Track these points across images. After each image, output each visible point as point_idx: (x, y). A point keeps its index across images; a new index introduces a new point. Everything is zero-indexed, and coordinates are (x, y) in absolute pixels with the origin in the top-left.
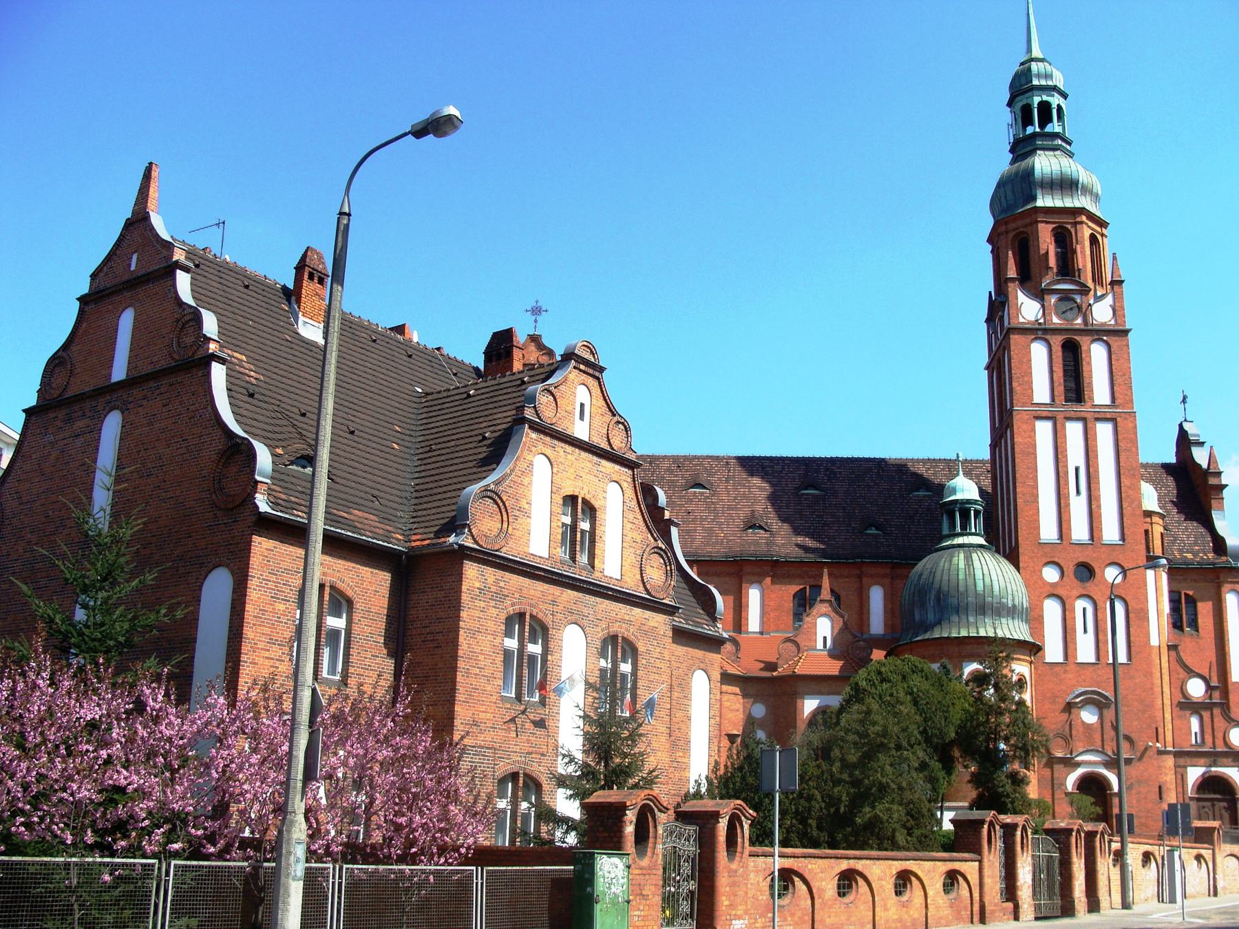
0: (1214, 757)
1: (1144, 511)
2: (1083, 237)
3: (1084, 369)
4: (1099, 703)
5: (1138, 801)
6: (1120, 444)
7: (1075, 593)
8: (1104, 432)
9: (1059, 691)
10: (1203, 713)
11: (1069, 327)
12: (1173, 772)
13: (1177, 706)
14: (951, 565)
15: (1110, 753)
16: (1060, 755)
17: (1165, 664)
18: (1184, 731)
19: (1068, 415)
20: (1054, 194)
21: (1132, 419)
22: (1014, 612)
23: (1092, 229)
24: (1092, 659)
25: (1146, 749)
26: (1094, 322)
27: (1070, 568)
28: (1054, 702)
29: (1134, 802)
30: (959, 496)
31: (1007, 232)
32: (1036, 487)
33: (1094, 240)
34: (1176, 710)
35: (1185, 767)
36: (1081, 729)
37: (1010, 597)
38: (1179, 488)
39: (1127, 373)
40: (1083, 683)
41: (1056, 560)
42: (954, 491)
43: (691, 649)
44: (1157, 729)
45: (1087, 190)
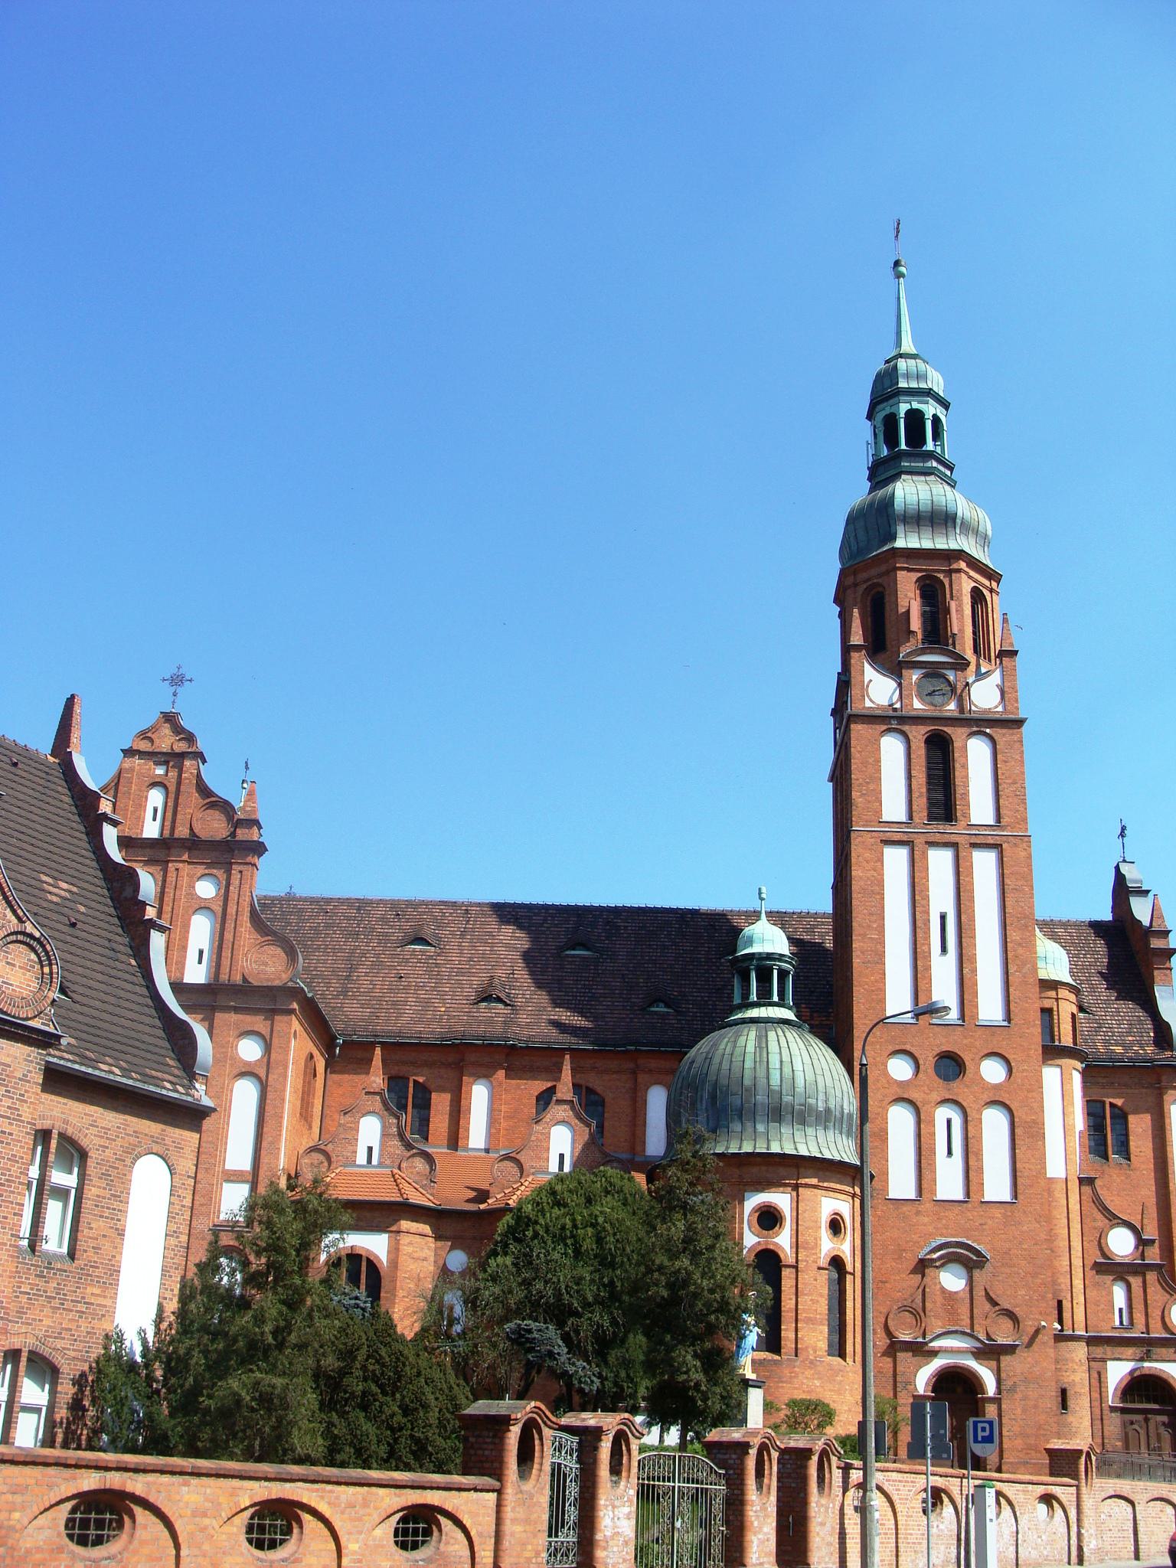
0: (1147, 1346)
1: (1041, 981)
2: (960, 590)
3: (957, 773)
4: (971, 1261)
5: (1024, 1411)
6: (1007, 881)
7: (936, 1096)
8: (984, 864)
9: (907, 1242)
10: (1131, 1279)
11: (937, 714)
12: (1085, 1368)
13: (1091, 1269)
14: (735, 1047)
15: (982, 1337)
16: (907, 1338)
17: (1075, 1206)
18: (1102, 1306)
20: (922, 532)
21: (1024, 845)
22: (825, 1118)
23: (976, 581)
24: (959, 1194)
25: (1037, 1332)
26: (973, 708)
27: (928, 1061)
28: (900, 1257)
29: (1019, 1411)
30: (756, 949)
31: (856, 585)
32: (882, 943)
33: (977, 596)
34: (1091, 1274)
35: (1104, 1360)
36: (939, 1299)
37: (821, 1097)
38: (1111, 956)
39: (1019, 780)
40: (944, 1231)
41: (908, 1047)
42: (750, 941)
43: (134, 1120)
44: (1060, 1303)
45: (967, 528)
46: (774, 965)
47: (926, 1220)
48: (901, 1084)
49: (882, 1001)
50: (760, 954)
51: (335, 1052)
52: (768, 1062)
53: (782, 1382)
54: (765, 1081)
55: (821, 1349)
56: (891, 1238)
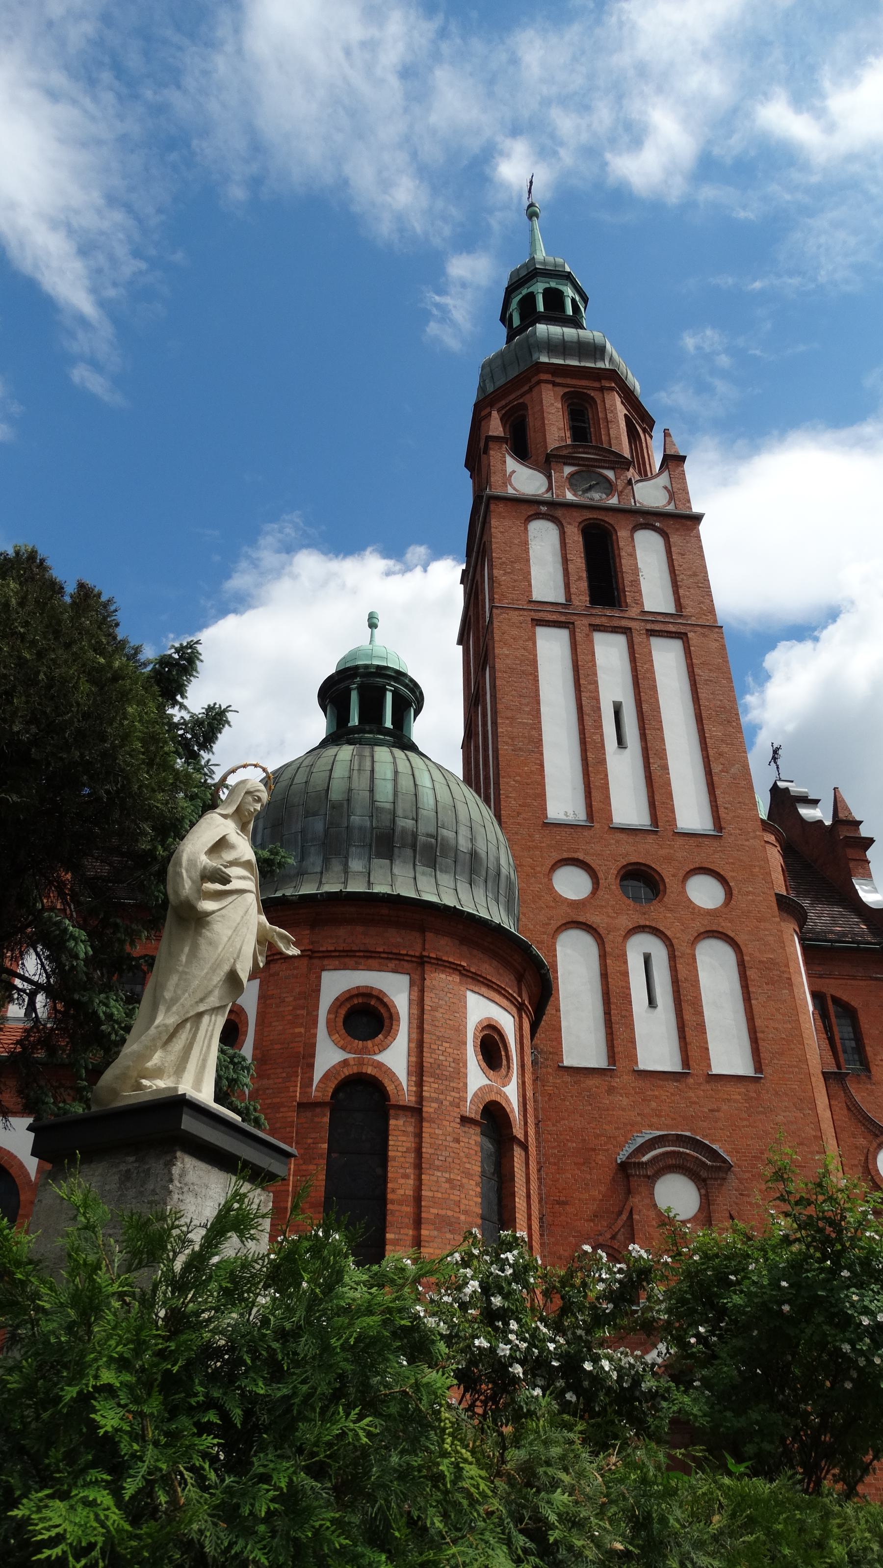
3: (623, 561)
7: (625, 922)
9: (597, 1136)
19: (597, 621)
37: (464, 831)
40: (655, 1120)
41: (580, 856)
47: (625, 1101)
48: (573, 904)
49: (541, 796)
50: (366, 667)
52: (372, 771)
54: (368, 793)
56: (571, 1129)
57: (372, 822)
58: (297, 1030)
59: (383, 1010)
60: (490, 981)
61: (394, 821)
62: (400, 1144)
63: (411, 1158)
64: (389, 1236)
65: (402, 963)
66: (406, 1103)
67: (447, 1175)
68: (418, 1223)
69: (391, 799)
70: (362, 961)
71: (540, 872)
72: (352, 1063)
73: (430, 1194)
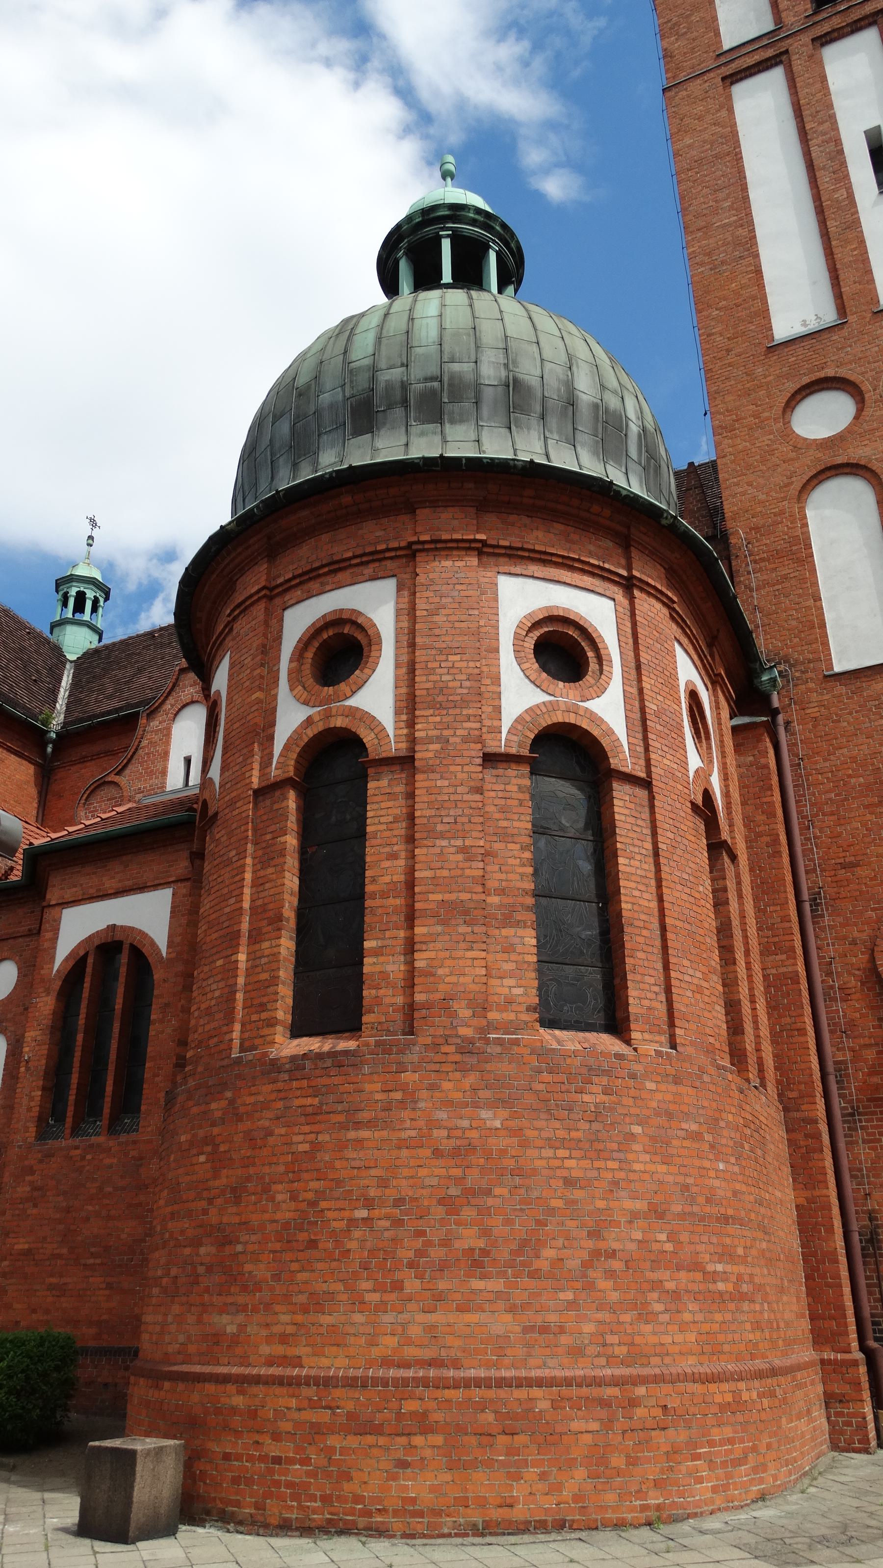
41: (830, 372)
46: (443, 229)
51: (45, 750)
53: (358, 1125)
55: (509, 1001)
56: (854, 759)
57: (344, 391)
58: (254, 697)
59: (360, 637)
60: (545, 553)
61: (373, 378)
62: (382, 813)
63: (401, 829)
64: (367, 944)
65: (384, 563)
66: (393, 753)
67: (459, 843)
68: (411, 919)
69: (370, 350)
70: (329, 579)
71: (768, 419)
72: (316, 719)
73: (428, 874)
